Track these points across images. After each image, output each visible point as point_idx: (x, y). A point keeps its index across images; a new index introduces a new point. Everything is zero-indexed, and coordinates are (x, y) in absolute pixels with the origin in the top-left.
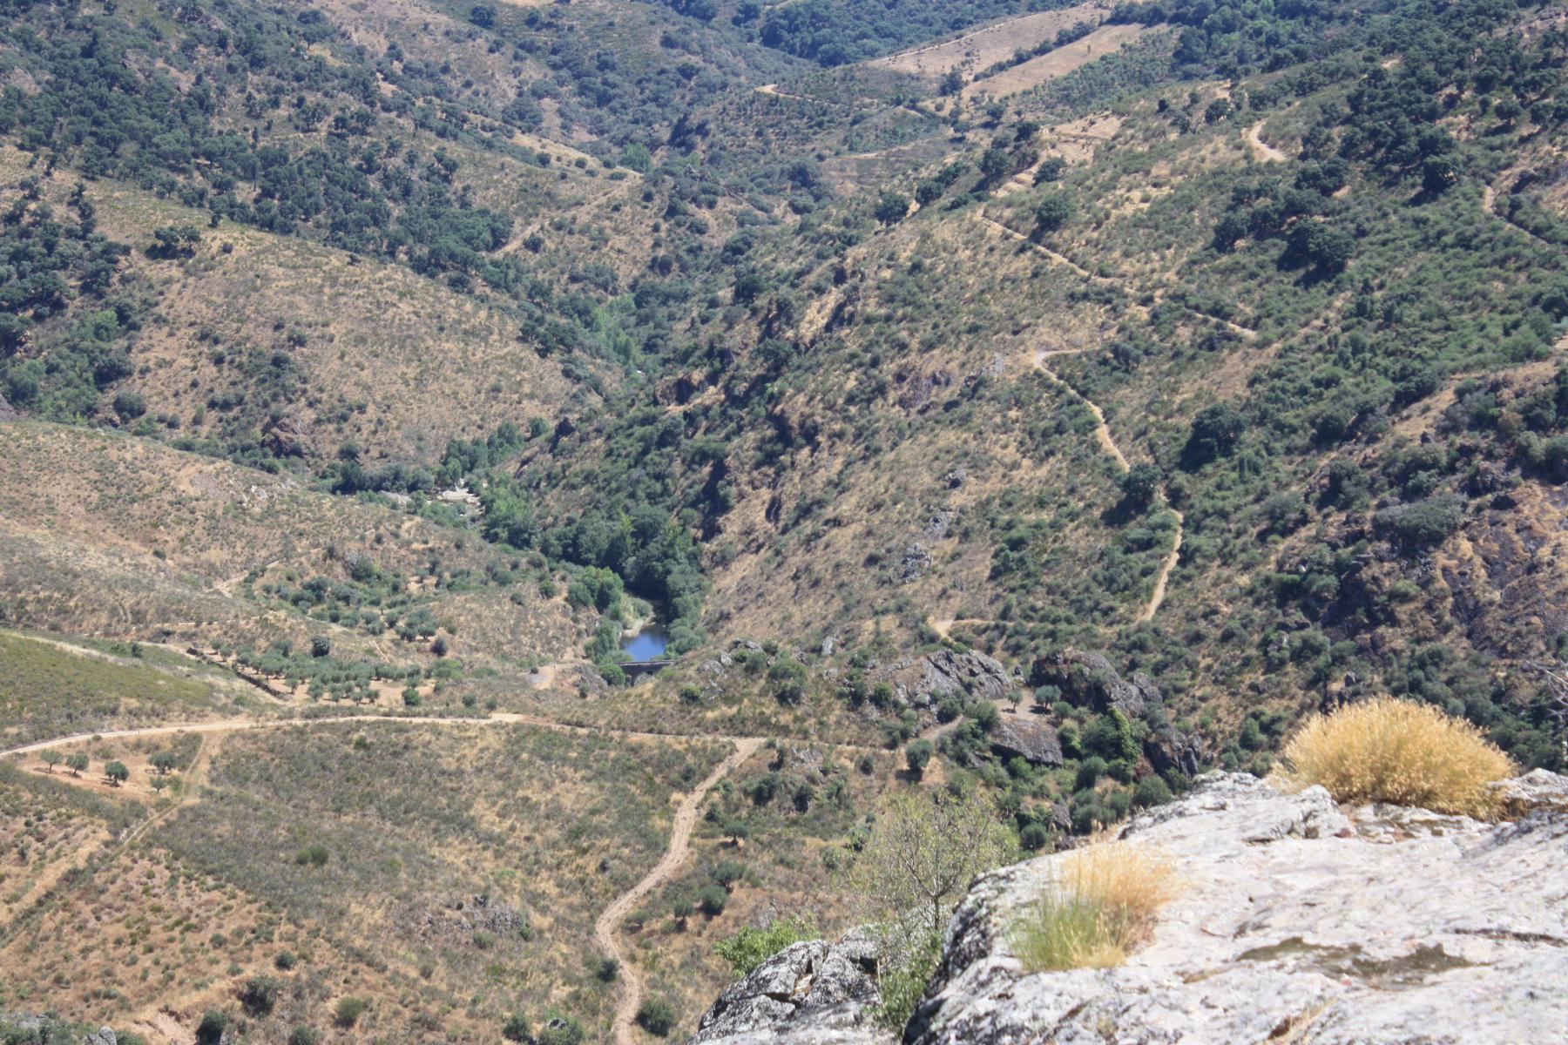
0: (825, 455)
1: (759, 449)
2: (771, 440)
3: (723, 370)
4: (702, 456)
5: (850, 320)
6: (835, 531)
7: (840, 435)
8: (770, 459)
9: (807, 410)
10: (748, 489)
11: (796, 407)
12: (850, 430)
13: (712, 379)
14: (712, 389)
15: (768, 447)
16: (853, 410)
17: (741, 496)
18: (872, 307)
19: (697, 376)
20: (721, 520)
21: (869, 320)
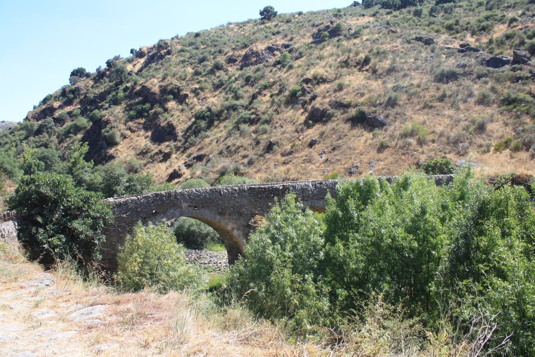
0: (195, 99)
1: (131, 110)
2: (137, 104)
3: (75, 98)
4: (77, 129)
5: (169, 53)
6: (323, 87)
7: (202, 89)
8: (140, 114)
9: (163, 84)
10: (128, 133)
11: (154, 85)
12: (209, 86)
13: (69, 102)
14: (69, 107)
15: (139, 107)
16: (203, 79)
17: (124, 137)
18: (179, 47)
19: (56, 104)
20: (111, 151)
21: (182, 51)
